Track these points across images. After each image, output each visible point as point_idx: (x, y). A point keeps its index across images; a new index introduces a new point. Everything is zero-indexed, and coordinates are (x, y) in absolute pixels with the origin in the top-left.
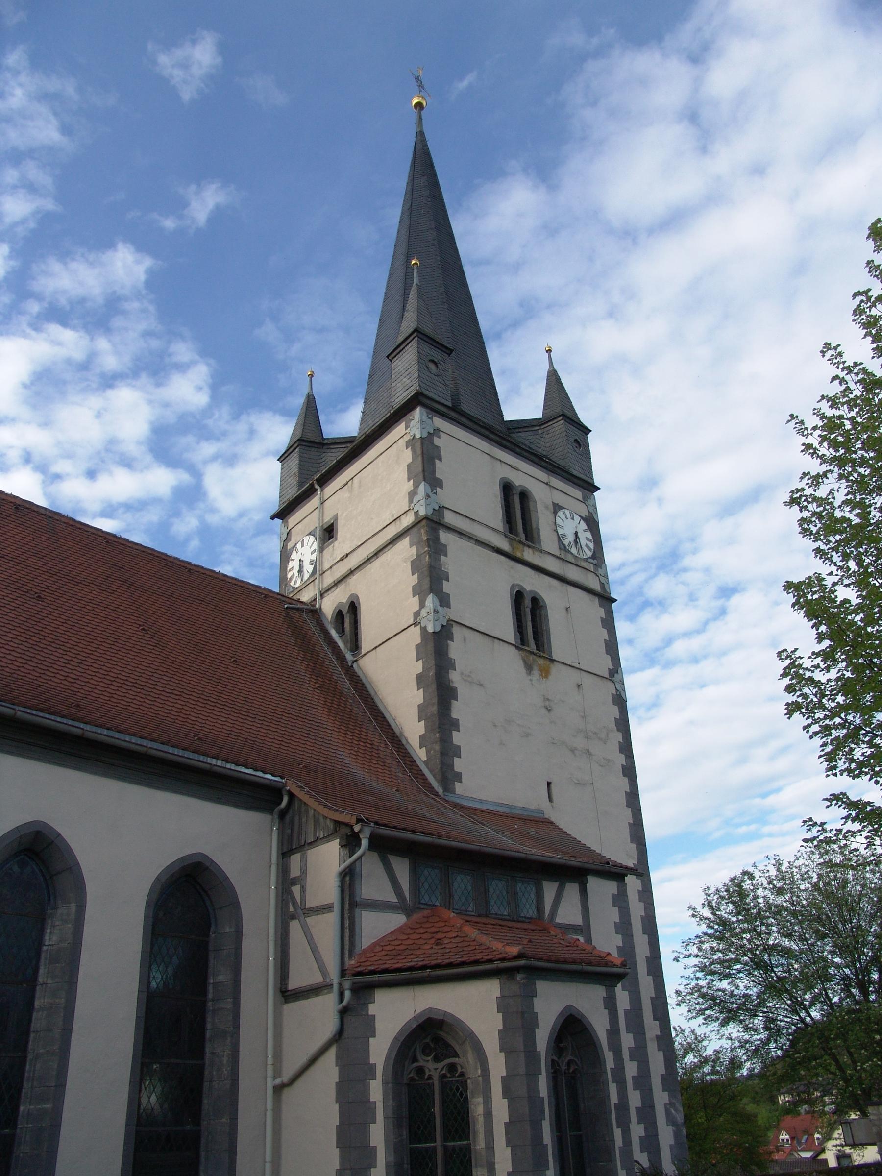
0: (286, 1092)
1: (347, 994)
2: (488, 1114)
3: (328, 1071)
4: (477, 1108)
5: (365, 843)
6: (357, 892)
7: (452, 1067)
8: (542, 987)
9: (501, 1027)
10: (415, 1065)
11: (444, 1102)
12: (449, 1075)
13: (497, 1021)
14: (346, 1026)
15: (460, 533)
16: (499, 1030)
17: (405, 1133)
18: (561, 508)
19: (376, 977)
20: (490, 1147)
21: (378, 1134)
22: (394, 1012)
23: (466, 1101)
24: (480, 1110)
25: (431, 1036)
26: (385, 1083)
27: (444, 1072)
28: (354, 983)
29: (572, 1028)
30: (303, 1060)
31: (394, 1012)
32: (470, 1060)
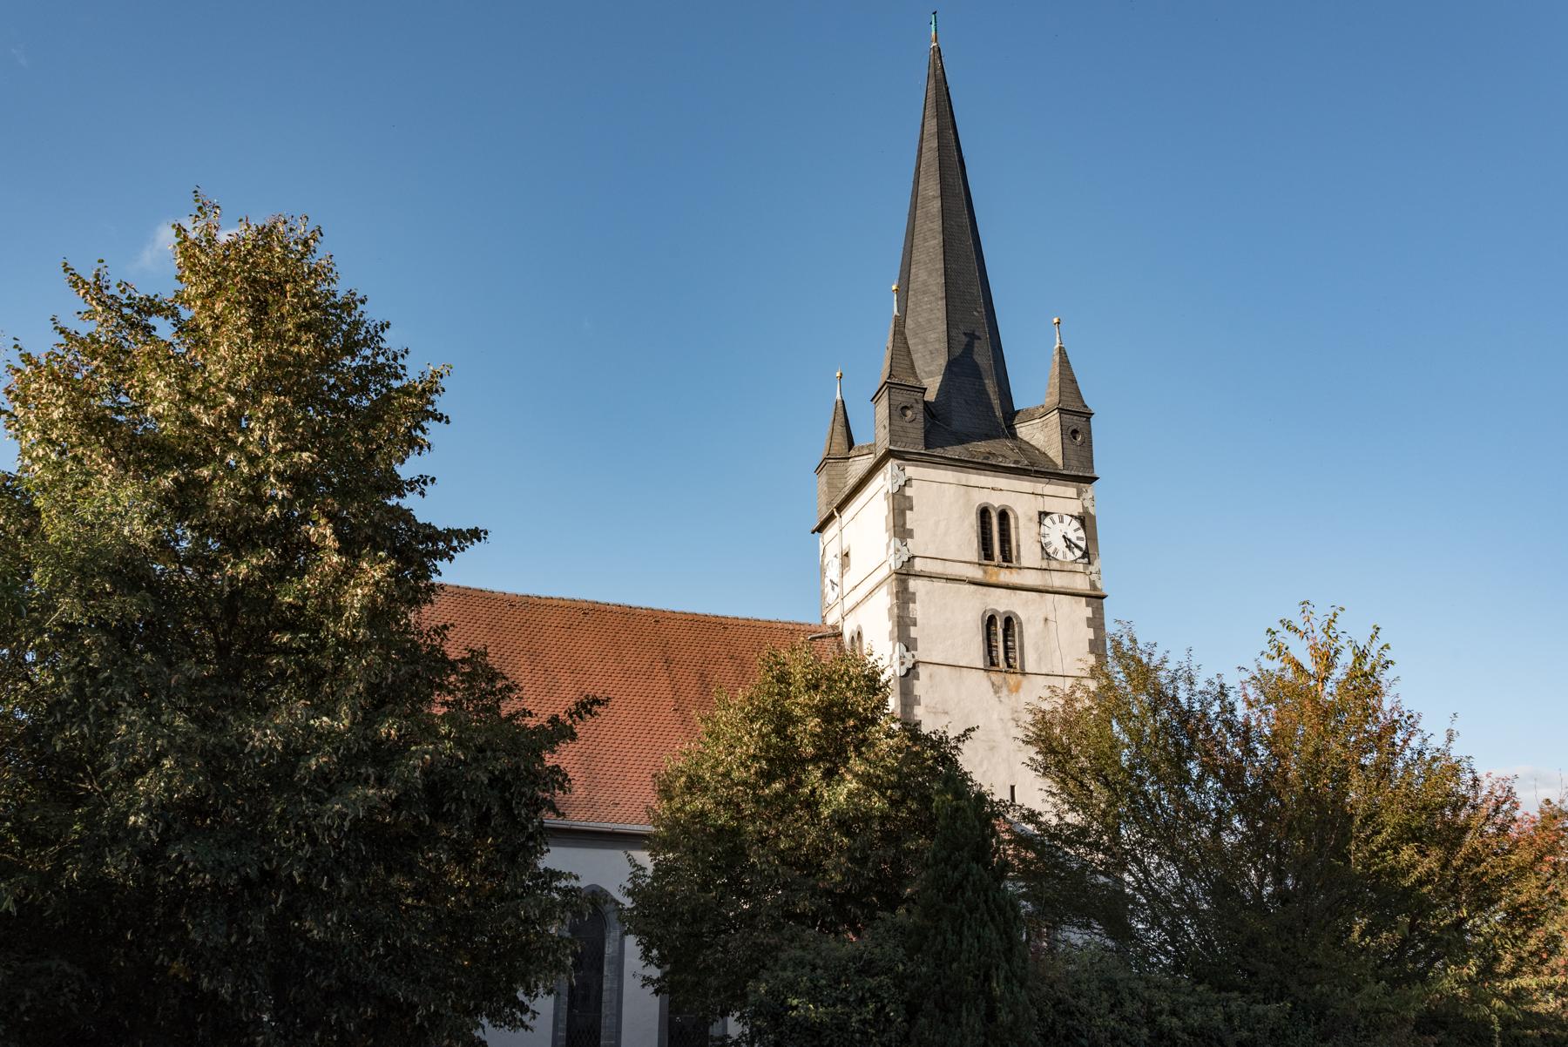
15: (930, 577)
18: (1047, 514)
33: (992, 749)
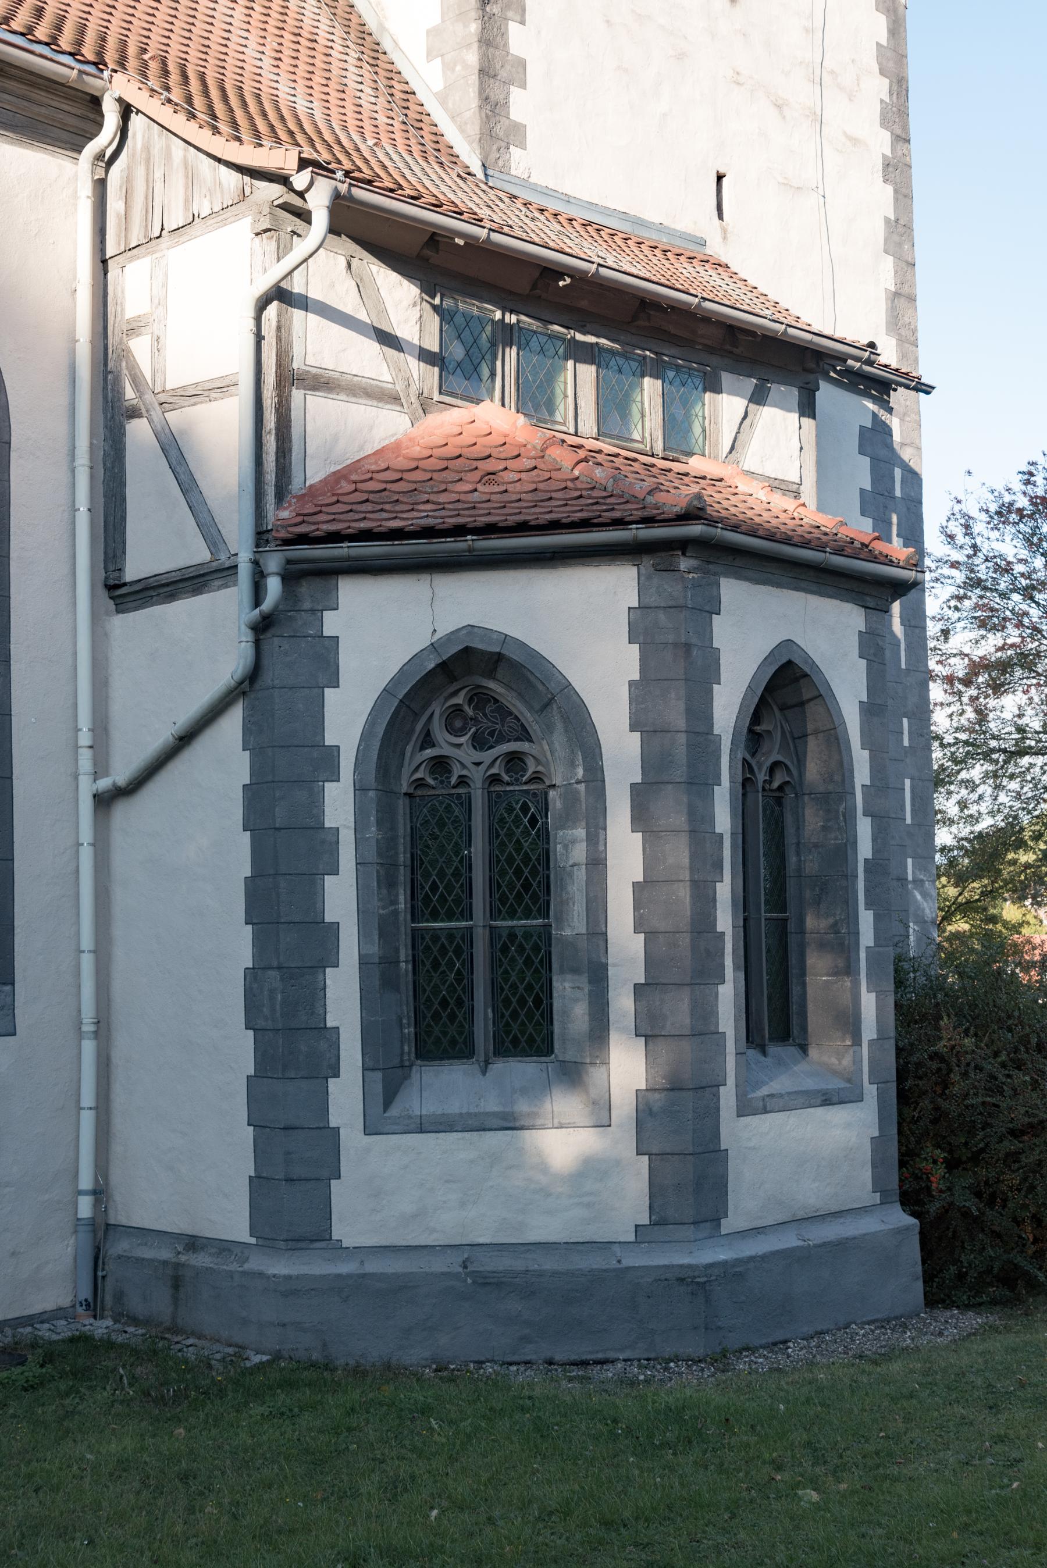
0: (122, 812)
1: (274, 586)
2: (597, 863)
3: (225, 758)
4: (571, 847)
5: (320, 219)
6: (297, 351)
7: (514, 760)
8: (733, 591)
9: (636, 676)
10: (429, 752)
11: (493, 834)
12: (506, 778)
13: (628, 661)
14: (266, 662)
16: (631, 683)
17: (402, 898)
19: (343, 550)
20: (598, 933)
21: (341, 898)
22: (381, 631)
23: (544, 835)
24: (579, 853)
25: (474, 687)
26: (359, 789)
27: (494, 770)
28: (289, 562)
29: (787, 687)
30: (162, 736)
31: (381, 631)
32: (557, 745)
33: (681, 56)
